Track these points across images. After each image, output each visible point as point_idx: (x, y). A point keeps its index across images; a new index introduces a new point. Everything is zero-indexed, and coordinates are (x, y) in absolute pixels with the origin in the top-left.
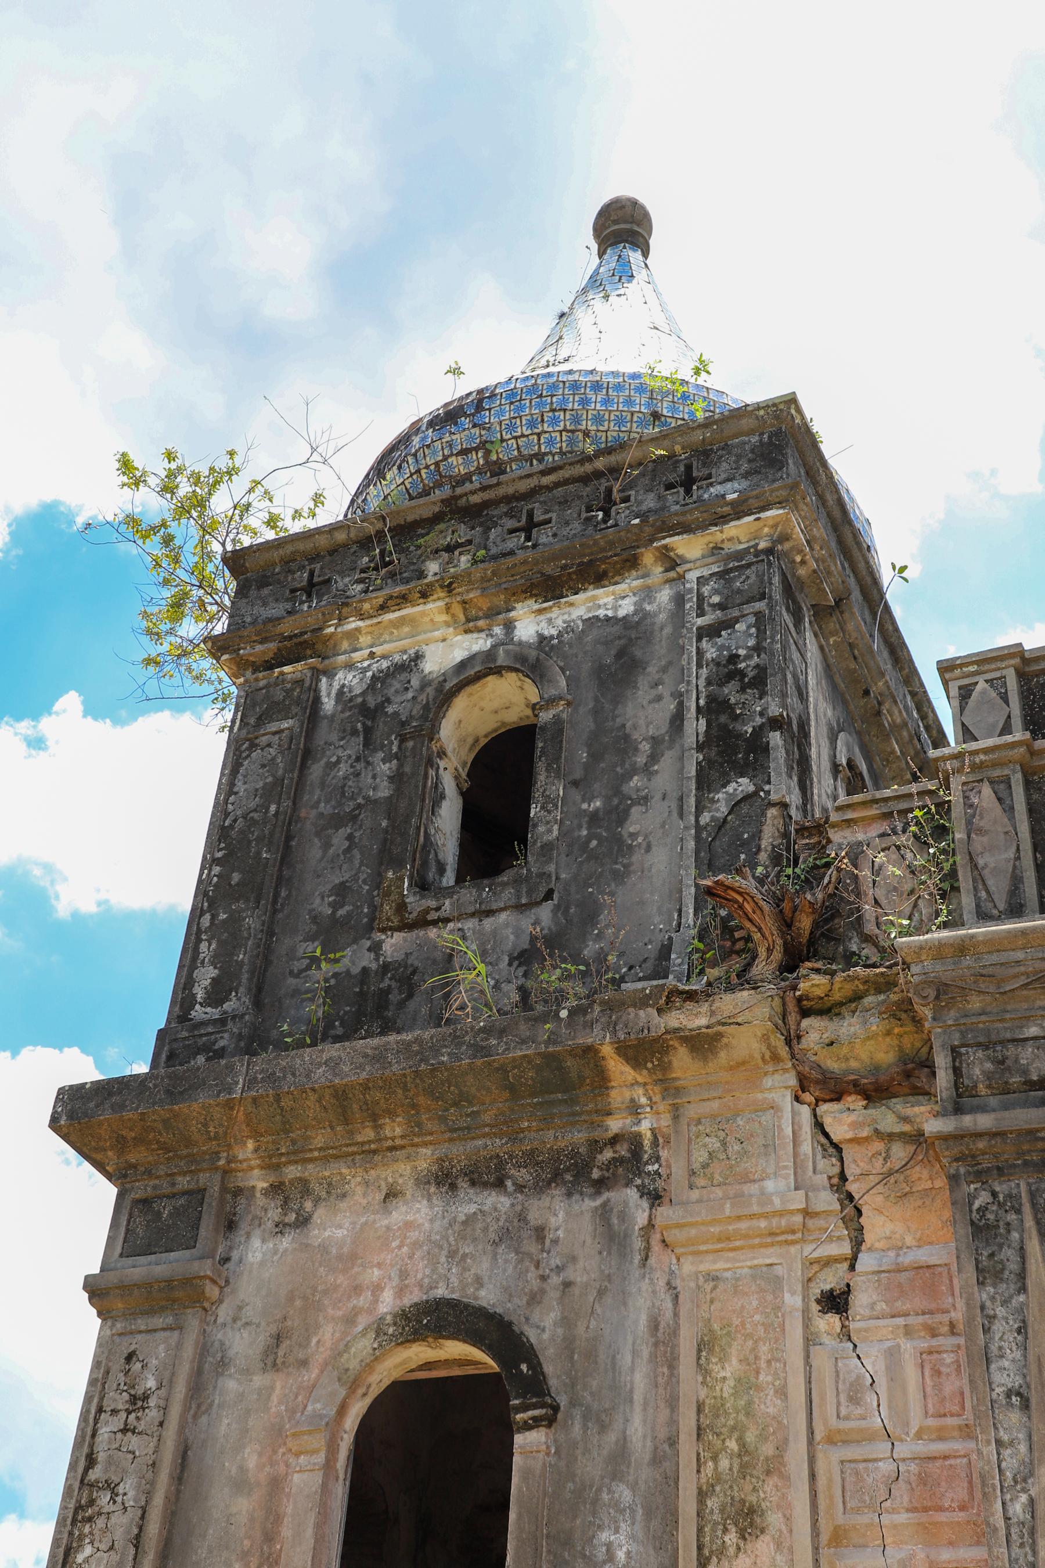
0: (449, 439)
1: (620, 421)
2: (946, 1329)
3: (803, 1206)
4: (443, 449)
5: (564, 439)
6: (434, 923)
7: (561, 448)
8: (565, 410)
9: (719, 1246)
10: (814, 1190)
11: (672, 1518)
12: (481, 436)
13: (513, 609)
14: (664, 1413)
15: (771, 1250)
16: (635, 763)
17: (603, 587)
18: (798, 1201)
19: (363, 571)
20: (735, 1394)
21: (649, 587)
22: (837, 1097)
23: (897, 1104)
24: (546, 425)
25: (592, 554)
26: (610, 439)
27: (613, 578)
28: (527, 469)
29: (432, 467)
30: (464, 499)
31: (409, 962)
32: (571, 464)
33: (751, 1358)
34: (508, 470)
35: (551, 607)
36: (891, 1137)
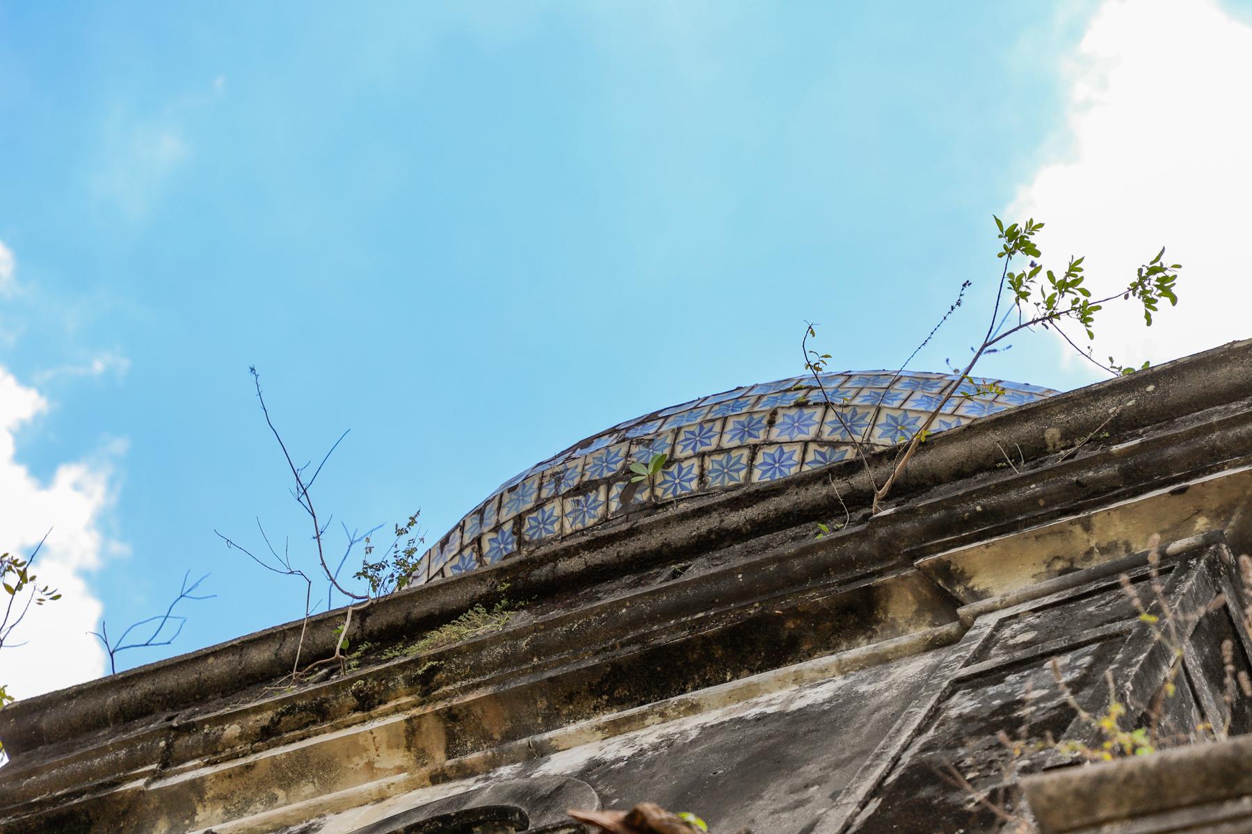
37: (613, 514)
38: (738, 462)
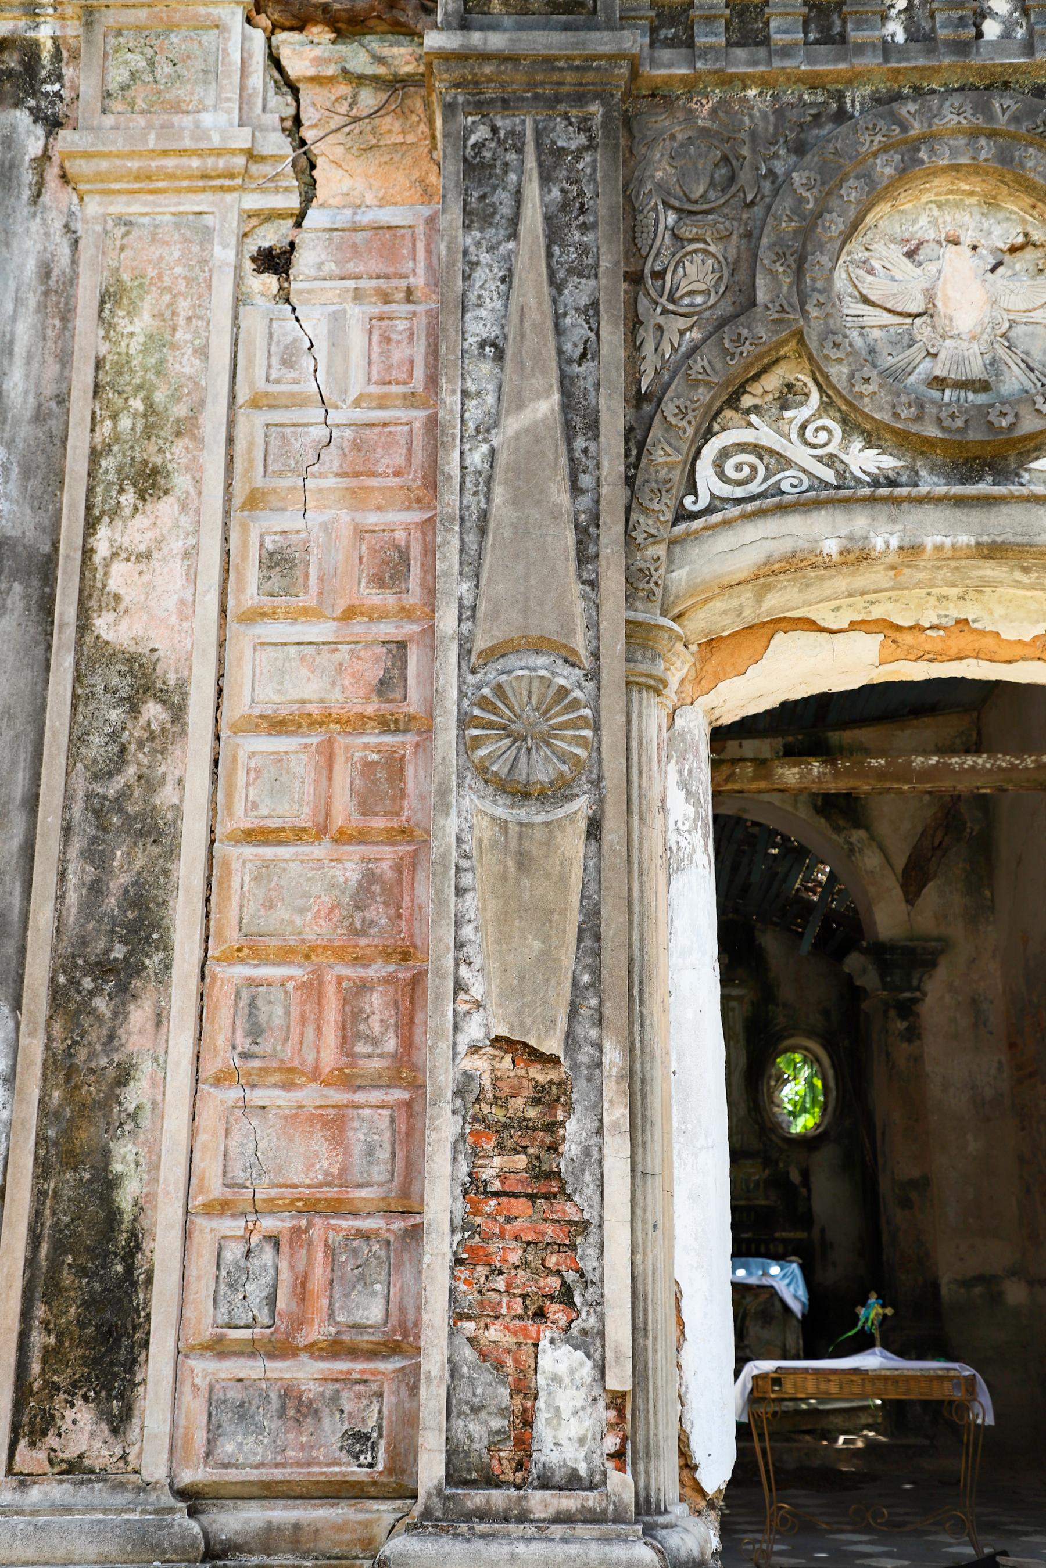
2: (402, 295)
3: (248, 145)
9: (137, 186)
10: (261, 130)
11: (57, 478)
14: (53, 369)
15: (202, 196)
18: (242, 139)
20: (145, 351)
22: (299, 26)
23: (373, 42)
33: (168, 314)
36: (360, 80)
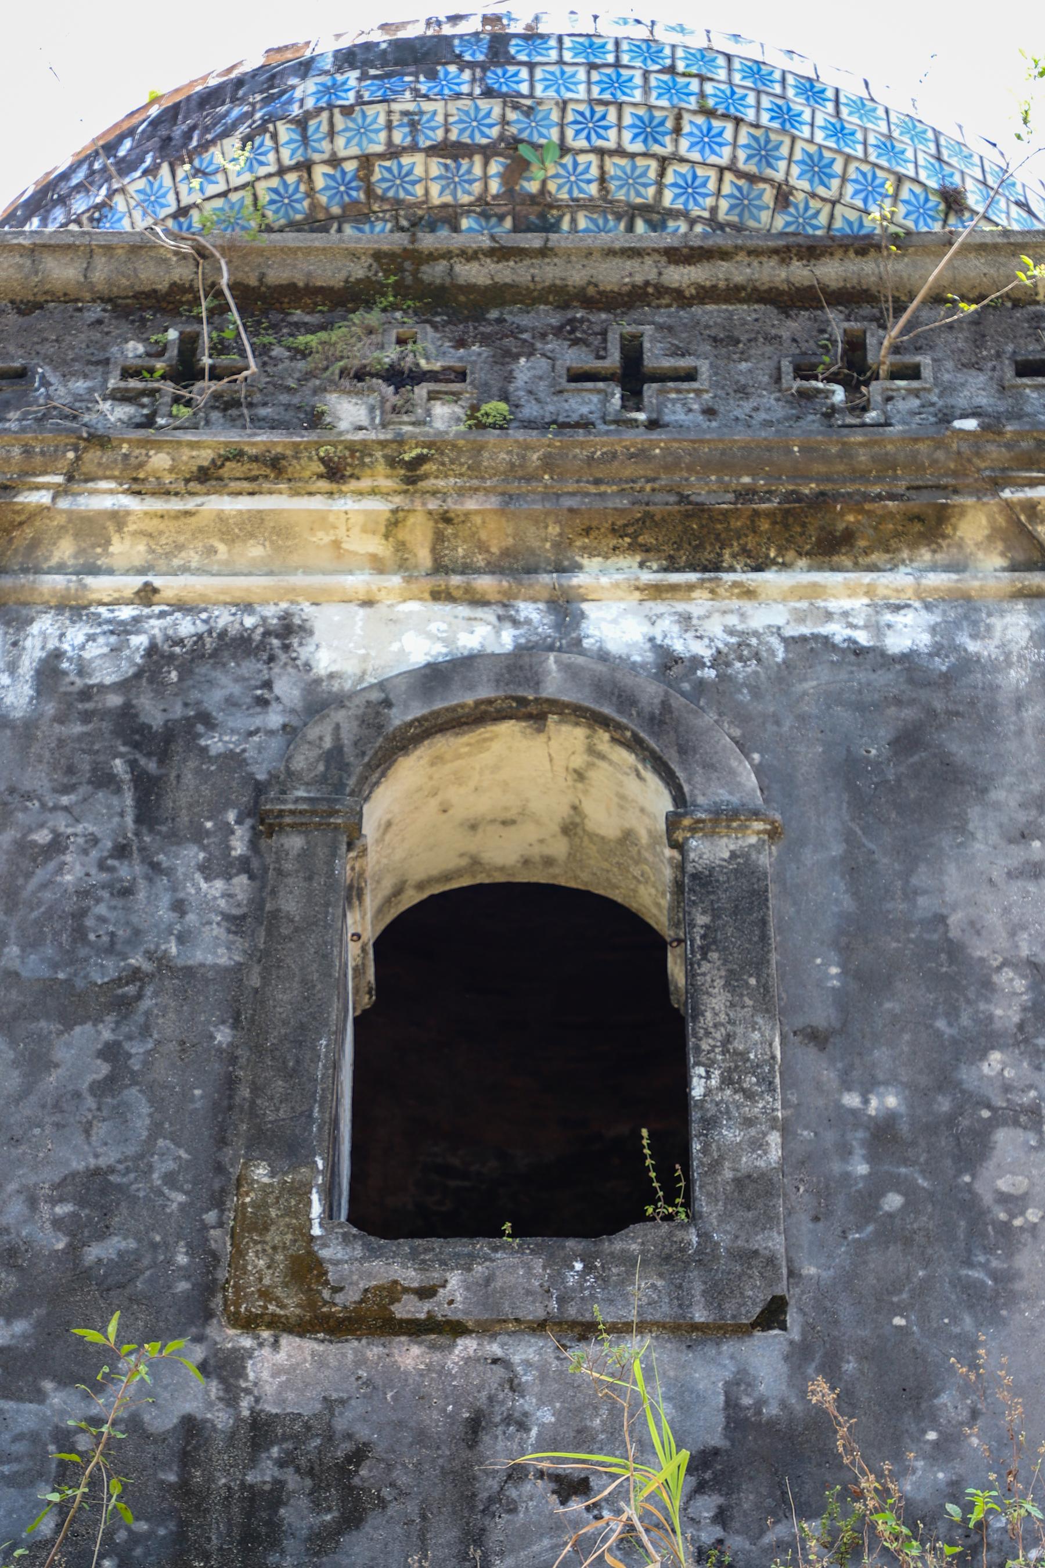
0: (411, 107)
1: (870, 189)
4: (389, 127)
5: (727, 189)
6: (416, 1329)
7: (714, 210)
8: (738, 121)
12: (504, 122)
13: (579, 567)
16: (990, 1018)
17: (833, 569)
19: (127, 373)
21: (967, 598)
24: (684, 144)
25: (828, 479)
26: (838, 224)
27: (866, 553)
28: (616, 235)
29: (350, 166)
30: (442, 266)
31: (340, 1424)
32: (753, 252)
34: (565, 225)
35: (691, 587)
37: (494, 197)
38: (644, 174)
